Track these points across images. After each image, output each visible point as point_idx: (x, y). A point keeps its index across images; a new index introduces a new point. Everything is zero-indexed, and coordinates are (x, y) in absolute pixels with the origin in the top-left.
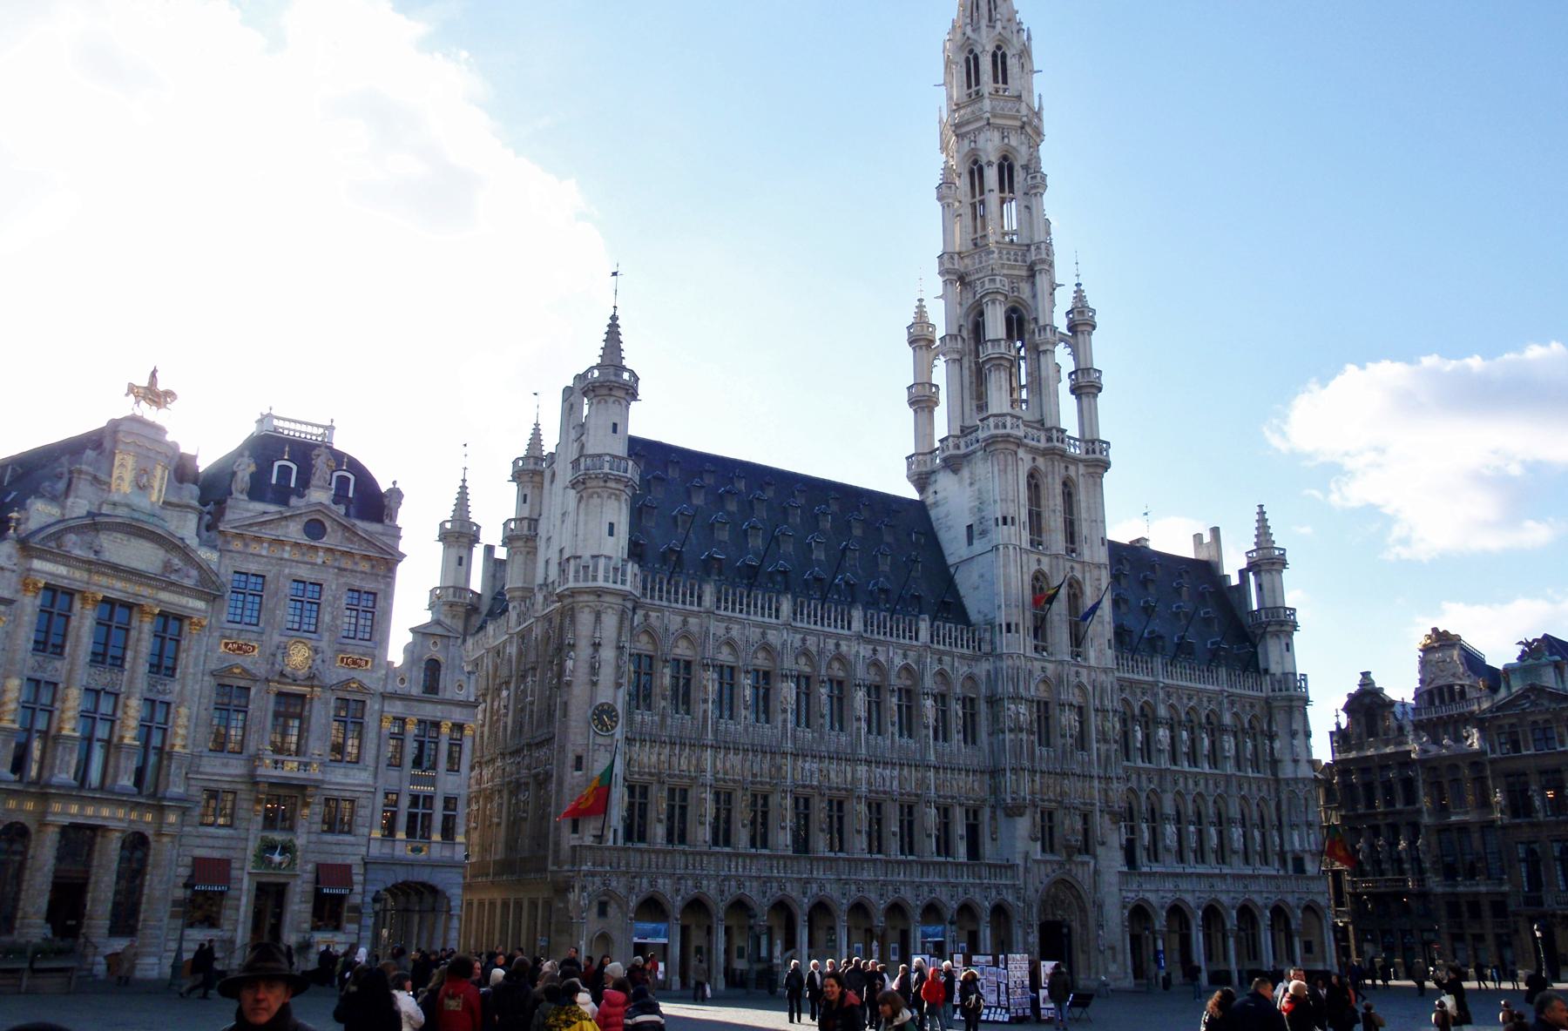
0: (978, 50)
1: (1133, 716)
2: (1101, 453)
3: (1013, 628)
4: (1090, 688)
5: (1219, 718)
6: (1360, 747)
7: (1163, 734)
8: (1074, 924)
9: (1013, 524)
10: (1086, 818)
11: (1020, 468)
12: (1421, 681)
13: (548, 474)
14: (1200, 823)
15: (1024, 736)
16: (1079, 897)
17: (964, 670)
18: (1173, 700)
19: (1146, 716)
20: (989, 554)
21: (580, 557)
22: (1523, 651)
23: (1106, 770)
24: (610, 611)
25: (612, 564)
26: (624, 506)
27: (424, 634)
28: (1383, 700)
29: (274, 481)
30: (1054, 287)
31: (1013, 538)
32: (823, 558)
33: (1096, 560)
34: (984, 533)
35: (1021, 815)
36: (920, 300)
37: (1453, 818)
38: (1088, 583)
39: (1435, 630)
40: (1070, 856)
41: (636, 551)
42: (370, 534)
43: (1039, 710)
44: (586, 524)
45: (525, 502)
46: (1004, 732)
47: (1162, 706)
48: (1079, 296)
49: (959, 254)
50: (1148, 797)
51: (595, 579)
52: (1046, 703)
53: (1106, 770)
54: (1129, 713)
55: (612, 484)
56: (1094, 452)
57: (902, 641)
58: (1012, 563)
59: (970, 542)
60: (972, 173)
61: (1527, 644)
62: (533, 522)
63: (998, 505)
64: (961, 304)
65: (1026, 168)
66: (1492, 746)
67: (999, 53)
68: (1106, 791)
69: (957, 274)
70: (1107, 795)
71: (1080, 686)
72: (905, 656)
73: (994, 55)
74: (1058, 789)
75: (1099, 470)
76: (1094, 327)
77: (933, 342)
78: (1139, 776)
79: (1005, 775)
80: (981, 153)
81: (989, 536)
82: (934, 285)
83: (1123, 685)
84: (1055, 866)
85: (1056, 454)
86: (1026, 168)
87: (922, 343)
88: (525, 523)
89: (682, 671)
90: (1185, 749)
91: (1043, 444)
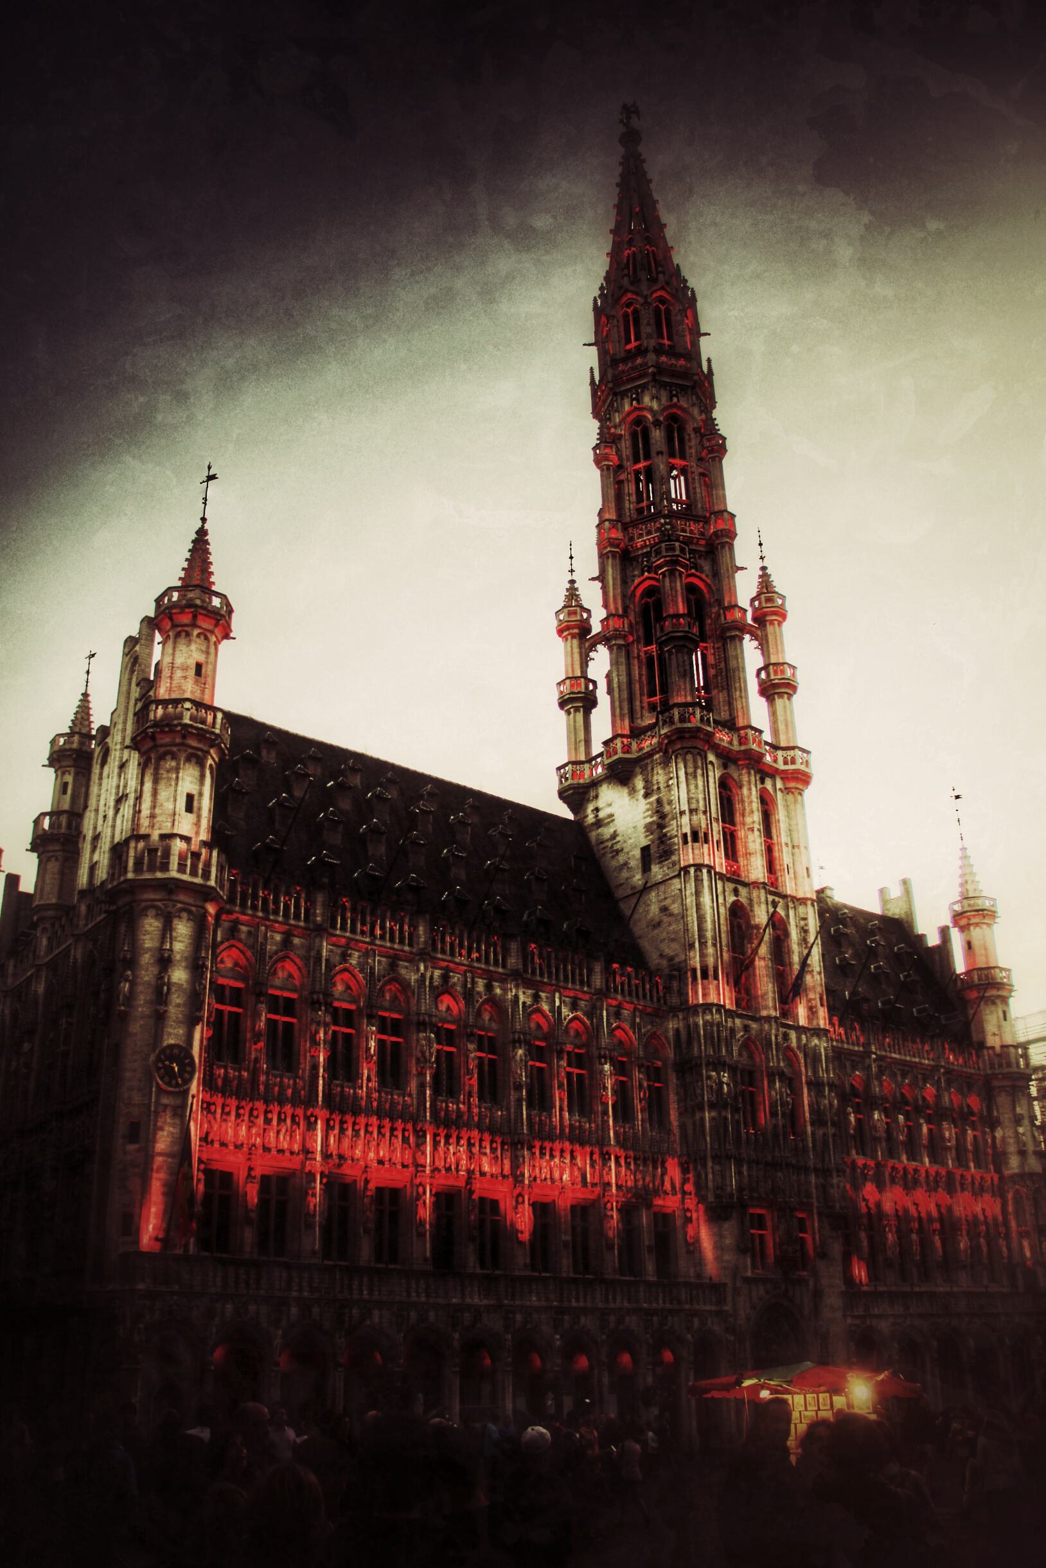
3: (711, 972)
4: (801, 1055)
9: (706, 841)
11: (711, 774)
20: (676, 881)
23: (823, 1161)
24: (184, 915)
31: (706, 858)
32: (463, 876)
33: (800, 895)
35: (726, 1219)
44: (155, 793)
45: (64, 792)
46: (702, 1109)
47: (876, 1083)
51: (165, 867)
53: (823, 1161)
55: (193, 743)
56: (793, 762)
58: (706, 890)
60: (634, 436)
75: (800, 786)
76: (784, 616)
77: (589, 630)
79: (705, 1166)
81: (674, 858)
82: (588, 563)
85: (753, 761)
87: (576, 631)
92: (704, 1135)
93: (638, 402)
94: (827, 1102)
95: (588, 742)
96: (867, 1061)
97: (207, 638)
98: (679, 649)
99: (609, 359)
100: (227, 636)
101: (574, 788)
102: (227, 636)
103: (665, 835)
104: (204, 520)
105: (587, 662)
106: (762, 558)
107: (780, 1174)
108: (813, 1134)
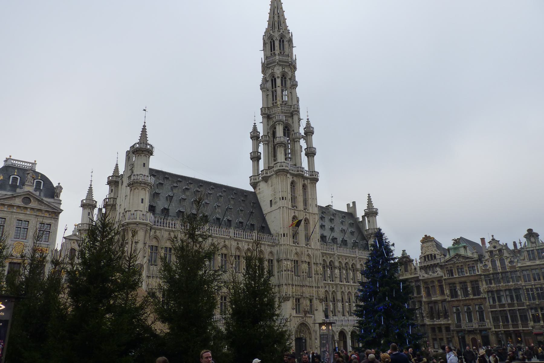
0: (274, 39)
1: (327, 266)
2: (315, 176)
5: (355, 265)
6: (403, 276)
7: (337, 271)
8: (307, 338)
10: (311, 301)
12: (422, 253)
13: (120, 181)
14: (350, 302)
15: (289, 273)
16: (309, 329)
17: (269, 249)
18: (340, 260)
19: (331, 265)
21: (130, 211)
22: (454, 242)
23: (318, 284)
24: (141, 230)
25: (141, 213)
26: (147, 192)
27: (70, 239)
28: (410, 260)
29: (10, 183)
30: (299, 120)
31: (286, 204)
32: (220, 211)
34: (276, 203)
35: (289, 300)
36: (255, 124)
37: (433, 299)
38: (311, 220)
39: (426, 236)
40: (305, 314)
41: (152, 209)
42: (49, 203)
43: (294, 263)
44: (133, 199)
45: (112, 192)
46: (283, 271)
48: (308, 123)
49: (268, 108)
50: (332, 294)
51: (136, 219)
52: (297, 261)
54: (325, 265)
55: (143, 185)
56: (313, 175)
57: (247, 240)
59: (271, 206)
61: (455, 240)
62: (115, 199)
63: (280, 193)
64: (268, 125)
65: (290, 79)
66: (445, 274)
67: (282, 40)
68: (317, 291)
69: (267, 115)
70: (318, 293)
71: (309, 255)
72: (248, 245)
73: (280, 41)
74: (301, 291)
77: (259, 138)
78: (329, 286)
80: (275, 74)
81: (278, 204)
82: (260, 118)
83: (323, 254)
84: (300, 318)
86: (290, 79)
88: (112, 200)
89: (168, 251)
90: (344, 277)
91: (296, 173)
92: (283, 278)
93: (273, 70)
94: (319, 269)
95: (258, 169)
96: (334, 256)
97: (146, 156)
98: (280, 146)
99: (265, 57)
100: (152, 155)
101: (254, 183)
102: (152, 154)
103: (276, 198)
104: (145, 122)
105: (258, 147)
106: (308, 116)
107: (304, 288)
108: (315, 277)
